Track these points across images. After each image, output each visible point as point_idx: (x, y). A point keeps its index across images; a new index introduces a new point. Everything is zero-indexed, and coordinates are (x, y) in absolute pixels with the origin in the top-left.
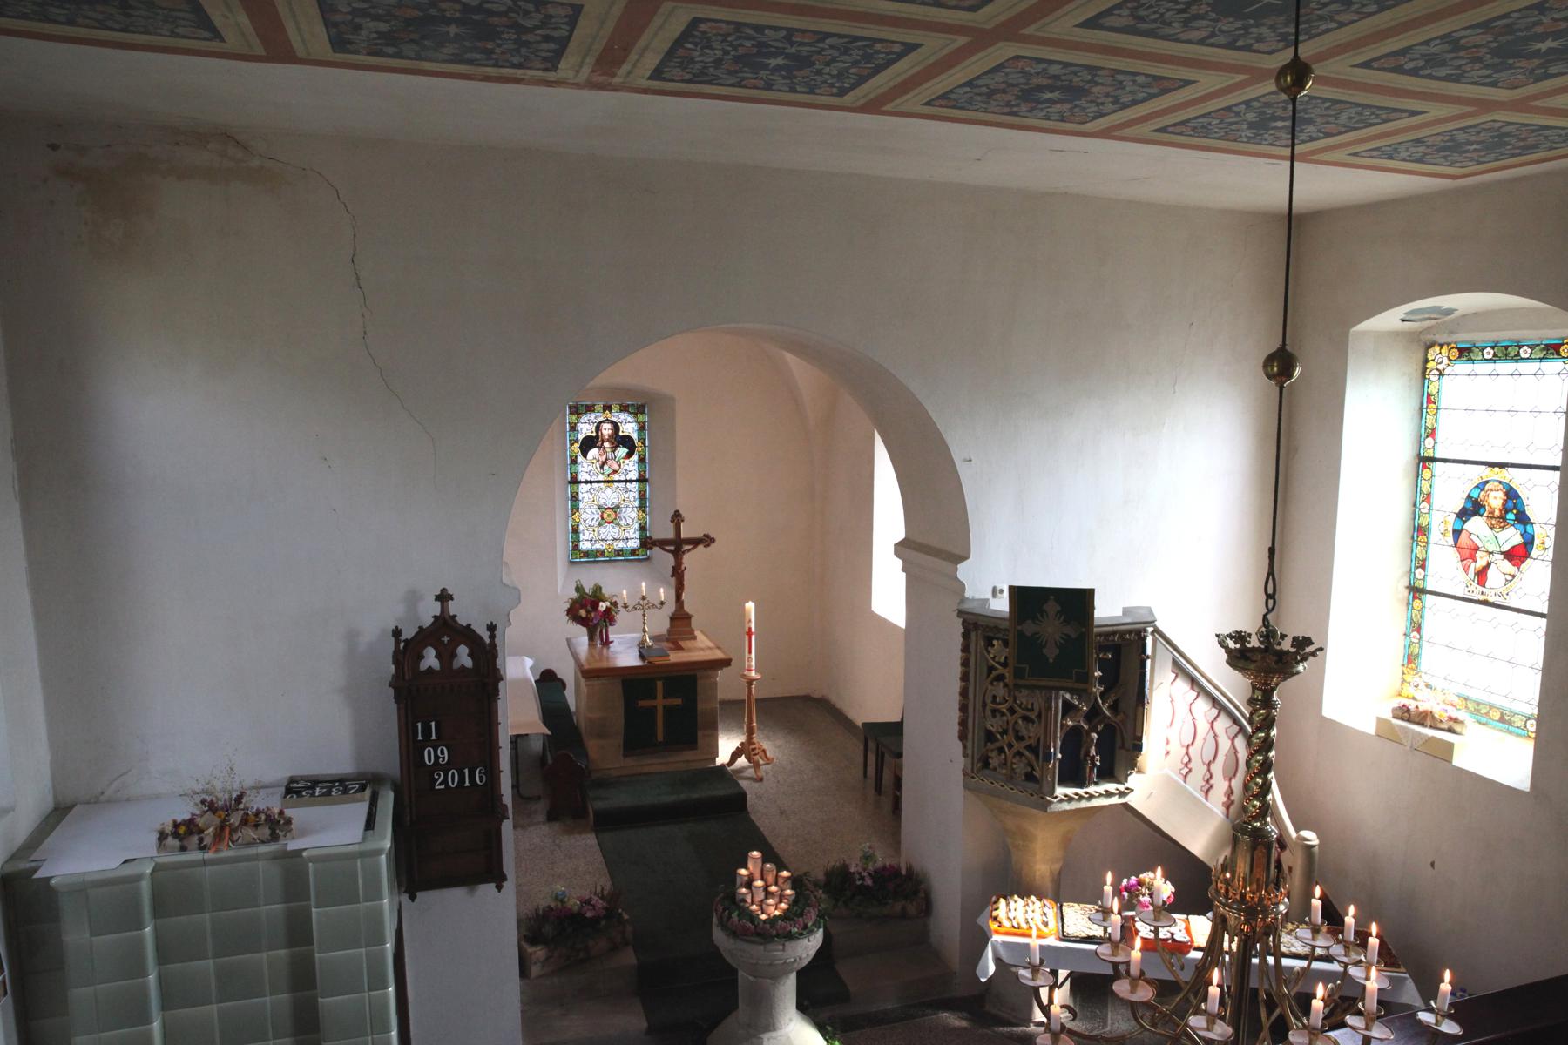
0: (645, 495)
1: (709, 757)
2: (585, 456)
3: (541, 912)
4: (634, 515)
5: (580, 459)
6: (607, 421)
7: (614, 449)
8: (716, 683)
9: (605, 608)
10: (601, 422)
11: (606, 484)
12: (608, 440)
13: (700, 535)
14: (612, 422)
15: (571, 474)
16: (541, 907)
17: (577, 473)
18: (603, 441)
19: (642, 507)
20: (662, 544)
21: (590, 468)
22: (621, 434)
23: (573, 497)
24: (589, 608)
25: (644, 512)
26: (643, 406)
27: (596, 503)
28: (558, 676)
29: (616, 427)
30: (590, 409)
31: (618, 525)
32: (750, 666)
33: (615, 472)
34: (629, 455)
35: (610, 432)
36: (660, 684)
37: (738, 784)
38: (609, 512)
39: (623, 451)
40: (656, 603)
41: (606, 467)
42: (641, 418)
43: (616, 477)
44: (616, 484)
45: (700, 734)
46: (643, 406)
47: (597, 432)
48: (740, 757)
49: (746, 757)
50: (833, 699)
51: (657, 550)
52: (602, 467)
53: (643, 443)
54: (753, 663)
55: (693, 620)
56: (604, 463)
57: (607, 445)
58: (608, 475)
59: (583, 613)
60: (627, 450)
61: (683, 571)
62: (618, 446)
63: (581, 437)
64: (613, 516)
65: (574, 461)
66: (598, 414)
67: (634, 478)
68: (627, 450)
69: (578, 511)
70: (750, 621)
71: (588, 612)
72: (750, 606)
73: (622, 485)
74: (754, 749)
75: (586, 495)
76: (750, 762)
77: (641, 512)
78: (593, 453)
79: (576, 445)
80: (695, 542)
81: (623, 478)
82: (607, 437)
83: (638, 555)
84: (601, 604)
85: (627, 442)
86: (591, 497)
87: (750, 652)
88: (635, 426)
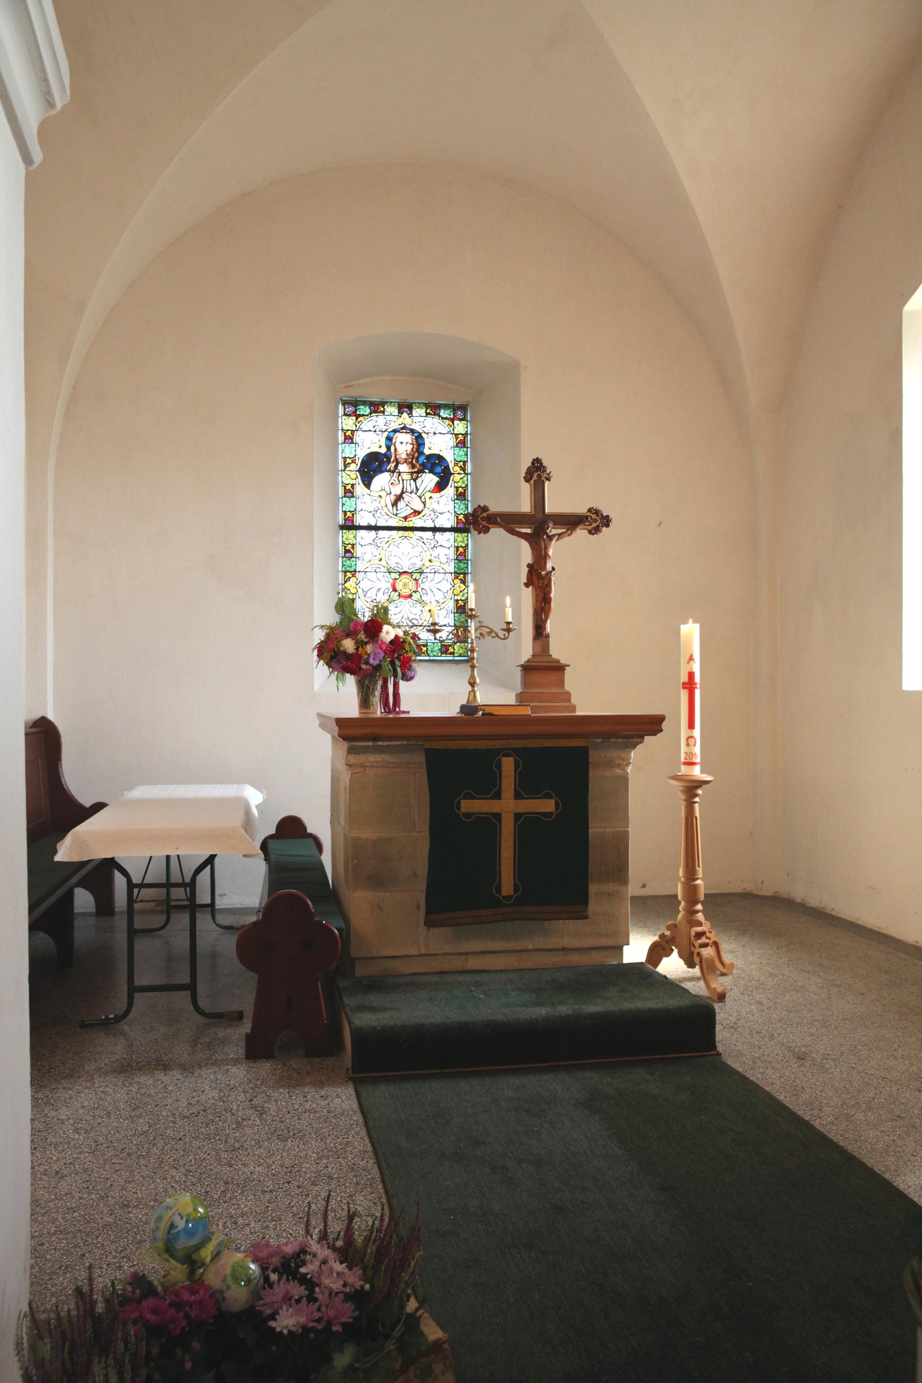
0: (464, 554)
1: (610, 942)
2: (368, 485)
3: (100, 1308)
4: (446, 586)
5: (360, 489)
6: (404, 429)
7: (415, 475)
8: (625, 779)
9: (392, 637)
10: (395, 431)
11: (401, 533)
12: (406, 461)
13: (582, 510)
14: (412, 431)
15: (345, 513)
16: (102, 1282)
17: (354, 513)
18: (398, 463)
19: (460, 575)
20: (510, 522)
21: (376, 504)
22: (427, 452)
23: (347, 551)
24: (362, 636)
25: (463, 582)
26: (463, 408)
27: (383, 563)
28: (310, 830)
29: (419, 440)
30: (376, 407)
31: (421, 602)
32: (690, 754)
33: (416, 513)
34: (440, 487)
35: (409, 447)
36: (508, 764)
37: (686, 991)
38: (405, 579)
39: (429, 480)
40: (498, 627)
41: (401, 504)
42: (460, 427)
43: (417, 522)
44: (418, 534)
45: (593, 888)
46: (463, 408)
47: (388, 448)
48: (668, 955)
49: (681, 955)
50: (799, 893)
51: (498, 533)
52: (395, 504)
53: (463, 469)
54: (697, 750)
55: (568, 671)
56: (399, 498)
57: (403, 468)
58: (406, 518)
59: (349, 645)
60: (436, 479)
61: (549, 573)
62: (421, 471)
63: (361, 454)
64: (412, 585)
65: (349, 492)
66: (389, 418)
67: (448, 525)
68: (436, 479)
69: (354, 576)
70: (691, 659)
71: (360, 644)
72: (691, 631)
73: (429, 534)
74: (699, 935)
75: (369, 550)
76: (690, 964)
77: (457, 581)
78: (381, 480)
79: (353, 467)
80: (571, 522)
81: (430, 524)
82: (404, 456)
83: (453, 653)
84: (386, 628)
85: (436, 464)
86: (376, 552)
87: (691, 725)
88: (450, 441)
